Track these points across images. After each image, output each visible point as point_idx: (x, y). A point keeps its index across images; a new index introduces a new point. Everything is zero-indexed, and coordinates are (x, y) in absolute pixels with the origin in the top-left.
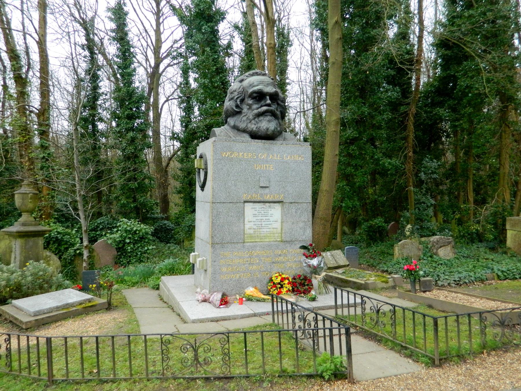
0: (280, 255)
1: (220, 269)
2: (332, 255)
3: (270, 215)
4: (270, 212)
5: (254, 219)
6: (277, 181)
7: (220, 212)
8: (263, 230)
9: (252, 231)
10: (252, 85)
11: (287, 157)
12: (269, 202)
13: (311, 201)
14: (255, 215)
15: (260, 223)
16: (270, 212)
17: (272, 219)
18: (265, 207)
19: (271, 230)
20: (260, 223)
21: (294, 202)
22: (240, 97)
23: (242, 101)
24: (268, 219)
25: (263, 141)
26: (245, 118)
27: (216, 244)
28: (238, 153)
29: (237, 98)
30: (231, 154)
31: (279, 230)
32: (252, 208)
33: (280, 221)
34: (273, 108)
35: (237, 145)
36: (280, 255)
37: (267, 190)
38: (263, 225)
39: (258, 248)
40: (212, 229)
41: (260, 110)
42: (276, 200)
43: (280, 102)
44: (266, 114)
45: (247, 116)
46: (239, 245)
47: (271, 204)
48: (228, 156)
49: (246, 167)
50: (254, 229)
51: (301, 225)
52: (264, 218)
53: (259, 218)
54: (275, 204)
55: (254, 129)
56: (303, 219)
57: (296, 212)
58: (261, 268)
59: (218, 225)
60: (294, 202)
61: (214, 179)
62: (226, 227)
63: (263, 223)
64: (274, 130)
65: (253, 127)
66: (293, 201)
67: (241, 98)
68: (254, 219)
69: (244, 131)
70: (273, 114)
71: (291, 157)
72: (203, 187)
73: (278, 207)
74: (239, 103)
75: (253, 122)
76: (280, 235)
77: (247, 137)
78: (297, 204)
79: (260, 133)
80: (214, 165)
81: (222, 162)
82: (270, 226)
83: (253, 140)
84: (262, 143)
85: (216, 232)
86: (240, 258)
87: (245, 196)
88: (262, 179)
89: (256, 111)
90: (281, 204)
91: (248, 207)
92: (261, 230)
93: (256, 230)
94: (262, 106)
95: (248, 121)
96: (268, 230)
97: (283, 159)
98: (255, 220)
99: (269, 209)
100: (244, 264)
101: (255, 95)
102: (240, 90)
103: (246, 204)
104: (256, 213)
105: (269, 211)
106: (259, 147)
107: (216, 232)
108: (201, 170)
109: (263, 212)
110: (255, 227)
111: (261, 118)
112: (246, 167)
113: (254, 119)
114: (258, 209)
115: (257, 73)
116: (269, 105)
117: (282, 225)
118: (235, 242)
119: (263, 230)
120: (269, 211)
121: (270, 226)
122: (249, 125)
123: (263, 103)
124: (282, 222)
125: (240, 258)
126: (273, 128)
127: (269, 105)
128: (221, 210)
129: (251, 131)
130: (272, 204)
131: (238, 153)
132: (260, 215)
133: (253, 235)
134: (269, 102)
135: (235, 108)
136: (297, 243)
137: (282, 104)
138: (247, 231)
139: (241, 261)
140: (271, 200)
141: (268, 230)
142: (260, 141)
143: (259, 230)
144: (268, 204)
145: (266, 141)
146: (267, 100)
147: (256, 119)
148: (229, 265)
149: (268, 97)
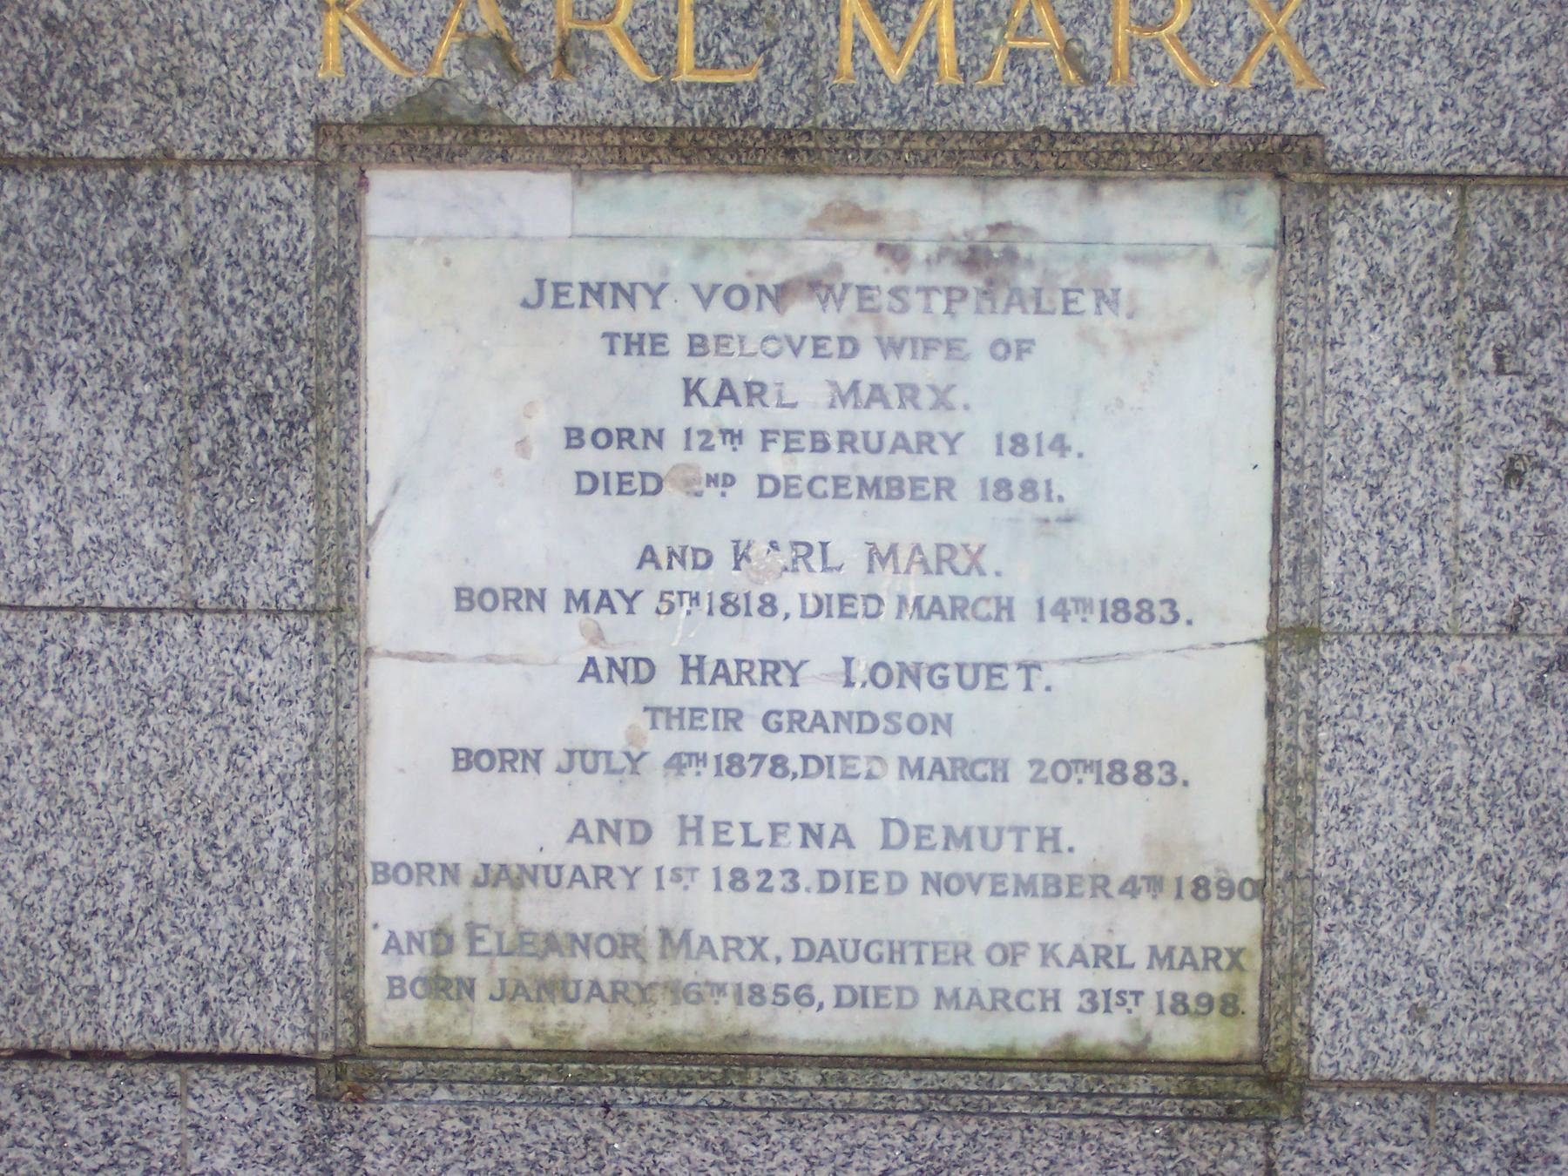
3: (979, 461)
5: (603, 544)
8: (819, 799)
9: (526, 819)
14: (609, 458)
16: (993, 399)
19: (1019, 801)
24: (944, 558)
32: (549, 294)
38: (817, 695)
47: (1024, 204)
50: (580, 759)
52: (846, 527)
53: (713, 522)
63: (821, 643)
68: (603, 544)
76: (1239, 923)
82: (981, 722)
90: (1261, 204)
92: (758, 800)
96: (930, 803)
99: (978, 328)
103: (404, 204)
104: (651, 391)
110: (610, 718)
114: (678, 317)
118: (122, 1025)
119: (819, 799)
121: (981, 722)
124: (1292, 639)
132: (746, 463)
133: (586, 911)
141: (930, 803)
143: (706, 795)
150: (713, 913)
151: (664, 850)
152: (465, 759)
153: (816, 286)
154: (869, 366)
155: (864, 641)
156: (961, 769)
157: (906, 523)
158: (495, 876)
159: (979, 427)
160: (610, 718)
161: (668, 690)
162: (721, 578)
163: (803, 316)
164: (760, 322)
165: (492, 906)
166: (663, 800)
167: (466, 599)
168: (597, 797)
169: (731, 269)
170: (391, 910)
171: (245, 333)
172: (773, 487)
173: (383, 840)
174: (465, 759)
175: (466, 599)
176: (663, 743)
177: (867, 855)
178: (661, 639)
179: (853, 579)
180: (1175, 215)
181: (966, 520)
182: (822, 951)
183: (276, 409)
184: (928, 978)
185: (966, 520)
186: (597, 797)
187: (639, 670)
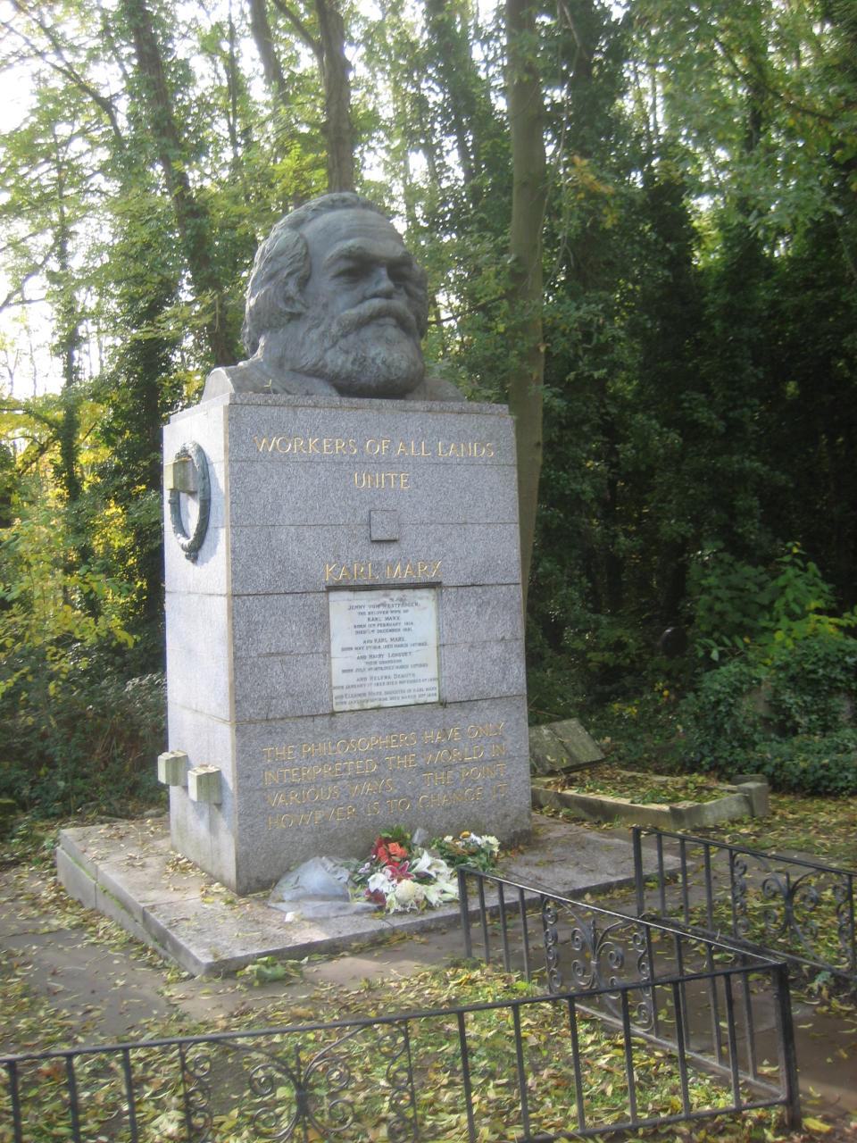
0: (438, 746)
1: (265, 799)
2: (554, 734)
3: (403, 626)
4: (404, 618)
6: (422, 523)
7: (257, 623)
8: (386, 672)
9: (352, 679)
10: (330, 234)
11: (446, 447)
12: (402, 587)
13: (519, 580)
14: (360, 629)
15: (376, 652)
16: (404, 618)
17: (409, 638)
18: (387, 600)
19: (410, 670)
20: (376, 652)
21: (473, 585)
25: (377, 402)
26: (314, 335)
27: (250, 722)
28: (306, 439)
29: (290, 274)
30: (283, 444)
31: (432, 672)
32: (351, 608)
33: (433, 642)
34: (399, 303)
35: (301, 416)
36: (438, 746)
37: (389, 553)
39: (374, 729)
40: (236, 678)
42: (420, 578)
43: (412, 287)
44: (381, 321)
45: (322, 328)
46: (318, 721)
47: (407, 593)
48: (275, 449)
50: (358, 670)
51: (496, 650)
52: (388, 636)
54: (419, 593)
55: (349, 366)
56: (499, 631)
57: (478, 613)
58: (385, 789)
59: (254, 665)
60: (473, 585)
61: (236, 525)
62: (277, 668)
63: (386, 651)
65: (338, 361)
66: (469, 582)
67: (301, 273)
69: (317, 373)
71: (458, 448)
72: (194, 552)
73: (426, 599)
74: (292, 288)
75: (342, 342)
76: (435, 684)
77: (325, 392)
78: (479, 590)
79: (363, 380)
80: (235, 478)
81: (258, 467)
83: (345, 400)
84: (371, 407)
85: (248, 685)
86: (324, 761)
87: (329, 569)
88: (376, 517)
91: (340, 605)
92: (379, 673)
93: (367, 674)
94: (364, 299)
95: (327, 344)
97: (435, 454)
98: (360, 643)
99: (402, 609)
100: (335, 781)
101: (344, 265)
103: (333, 596)
104: (364, 620)
105: (402, 615)
106: (367, 420)
107: (248, 685)
108: (183, 496)
109: (382, 617)
110: (362, 664)
111: (368, 332)
113: (344, 336)
114: (367, 610)
115: (344, 200)
116: (388, 295)
117: (439, 655)
118: (305, 713)
120: (402, 615)
121: (405, 660)
122: (329, 356)
123: (371, 288)
124: (441, 646)
125: (324, 761)
126: (404, 365)
127: (388, 295)
128: (261, 618)
130: (408, 593)
131: (306, 439)
132: (376, 628)
133: (360, 690)
134: (386, 284)
135: (282, 306)
136: (485, 704)
137: (421, 293)
138: (338, 679)
139: (326, 771)
140: (405, 579)
142: (366, 401)
143: (374, 673)
144: (396, 594)
145: (384, 402)
147: (351, 338)
148: (293, 785)
149: (383, 272)
150: (375, 689)
151: (368, 681)
152: (344, 671)
153: (384, 605)
154: (390, 615)
155: (391, 651)
156: (402, 667)
157: (395, 635)
158: (348, 687)
159: (403, 622)
160: (362, 664)
161: (368, 660)
162: (373, 644)
163: (381, 609)
164: (376, 610)
165: (347, 691)
166: (367, 674)
167: (343, 649)
168: (360, 675)
169: (372, 603)
170: (336, 693)
171: (318, 615)
172: (380, 631)
173: (334, 684)
174: (344, 671)
175: (343, 649)
176: (367, 667)
177: (393, 679)
178: (367, 653)
179: (389, 643)
180: (424, 593)
181: (402, 634)
182: (386, 693)
183: (321, 625)
184: (400, 695)
185: (402, 634)
186: (360, 675)
187: (364, 657)
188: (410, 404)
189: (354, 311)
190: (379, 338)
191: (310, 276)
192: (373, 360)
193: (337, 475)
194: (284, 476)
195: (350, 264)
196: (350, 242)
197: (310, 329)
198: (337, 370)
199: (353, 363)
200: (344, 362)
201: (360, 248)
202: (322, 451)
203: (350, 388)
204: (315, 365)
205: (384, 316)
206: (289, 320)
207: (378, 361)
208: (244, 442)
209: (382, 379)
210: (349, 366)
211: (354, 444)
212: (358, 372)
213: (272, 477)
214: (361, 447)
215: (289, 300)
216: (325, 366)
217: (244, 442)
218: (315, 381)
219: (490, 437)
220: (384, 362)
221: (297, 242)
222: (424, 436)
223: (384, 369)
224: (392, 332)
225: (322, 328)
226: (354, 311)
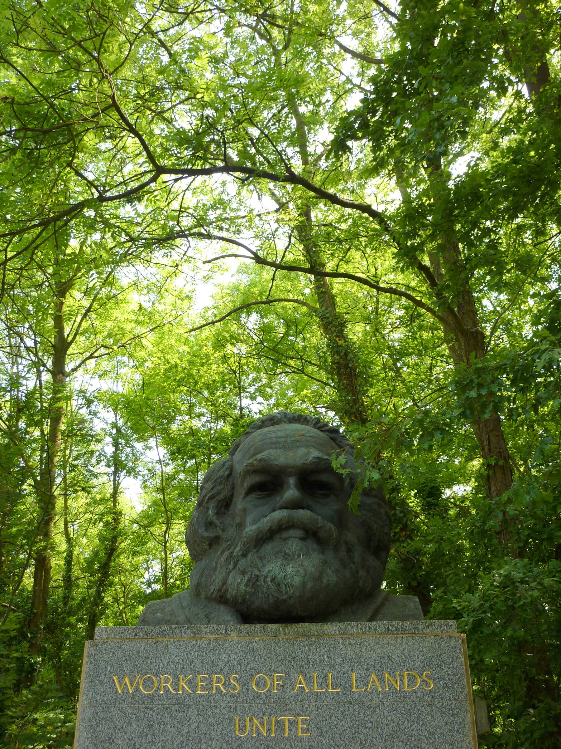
11: (363, 681)
22: (218, 493)
23: (226, 505)
25: (273, 627)
29: (211, 498)
35: (172, 649)
41: (259, 525)
44: (285, 535)
45: (231, 551)
49: (203, 729)
64: (304, 584)
65: (237, 584)
69: (222, 599)
70: (311, 534)
71: (381, 680)
75: (242, 563)
89: (250, 529)
94: (274, 510)
95: (231, 567)
97: (347, 689)
102: (221, 473)
106: (254, 650)
112: (203, 729)
113: (244, 555)
122: (230, 579)
126: (297, 580)
129: (236, 597)
131: (175, 676)
134: (291, 492)
142: (259, 626)
146: (288, 487)
149: (292, 481)
188: (314, 628)
189: (254, 527)
190: (277, 554)
191: (232, 496)
192: (266, 577)
193: (212, 720)
194: (145, 723)
195: (257, 479)
196: (259, 456)
197: (222, 553)
198: (234, 593)
199: (247, 585)
200: (239, 584)
201: (260, 460)
202: (194, 691)
203: (249, 614)
204: (220, 590)
205: (288, 528)
206: (210, 546)
207: (269, 580)
208: (101, 683)
209: (271, 601)
210: (243, 587)
211: (235, 679)
212: (252, 594)
213: (130, 724)
214: (246, 686)
215: (209, 525)
216: (227, 590)
217: (101, 683)
218: (222, 608)
219: (427, 664)
220: (273, 580)
221: (224, 465)
222: (332, 667)
223: (273, 587)
224: (293, 545)
225: (231, 551)
226: (254, 527)
